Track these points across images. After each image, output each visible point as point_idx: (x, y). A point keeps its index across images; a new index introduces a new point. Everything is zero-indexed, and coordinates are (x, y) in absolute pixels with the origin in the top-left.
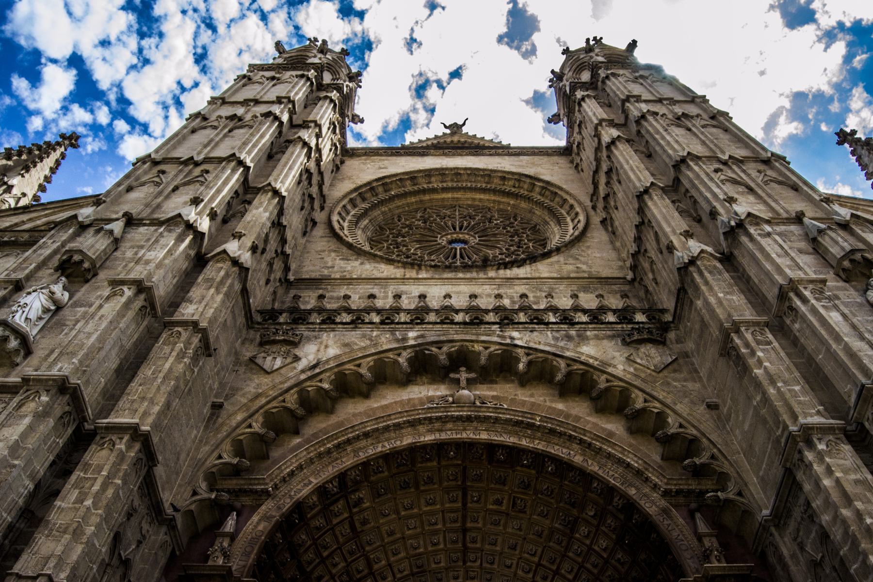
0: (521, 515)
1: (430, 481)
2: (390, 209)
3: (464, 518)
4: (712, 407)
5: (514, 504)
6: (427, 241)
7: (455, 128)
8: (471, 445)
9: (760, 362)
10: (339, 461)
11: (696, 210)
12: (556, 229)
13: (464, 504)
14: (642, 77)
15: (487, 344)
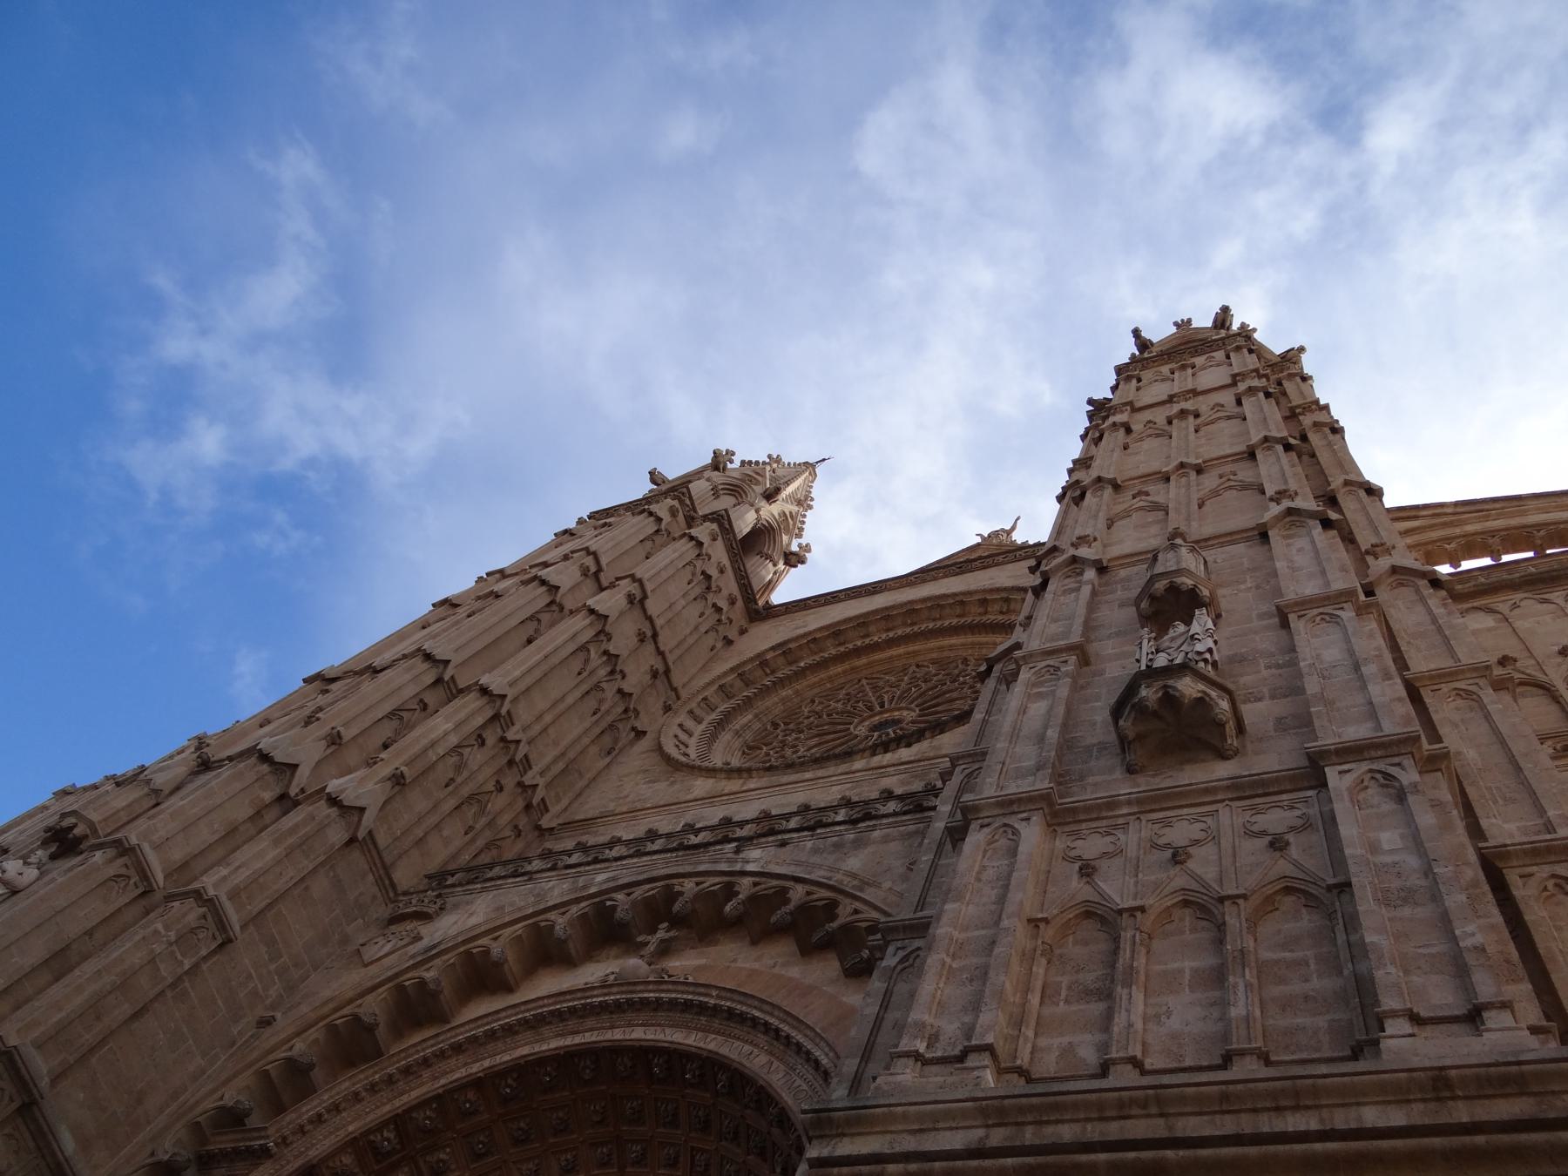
2: (797, 693)
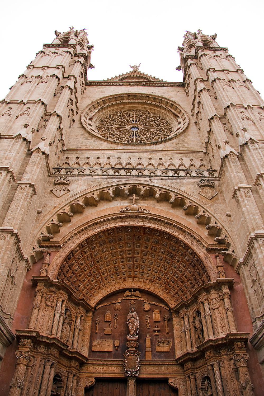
0: (155, 253)
1: (121, 239)
3: (133, 253)
4: (228, 215)
5: (152, 248)
6: (122, 128)
7: (136, 68)
8: (137, 227)
9: (245, 205)
10: (86, 234)
11: (232, 129)
13: (134, 248)
14: (217, 56)
15: (144, 185)
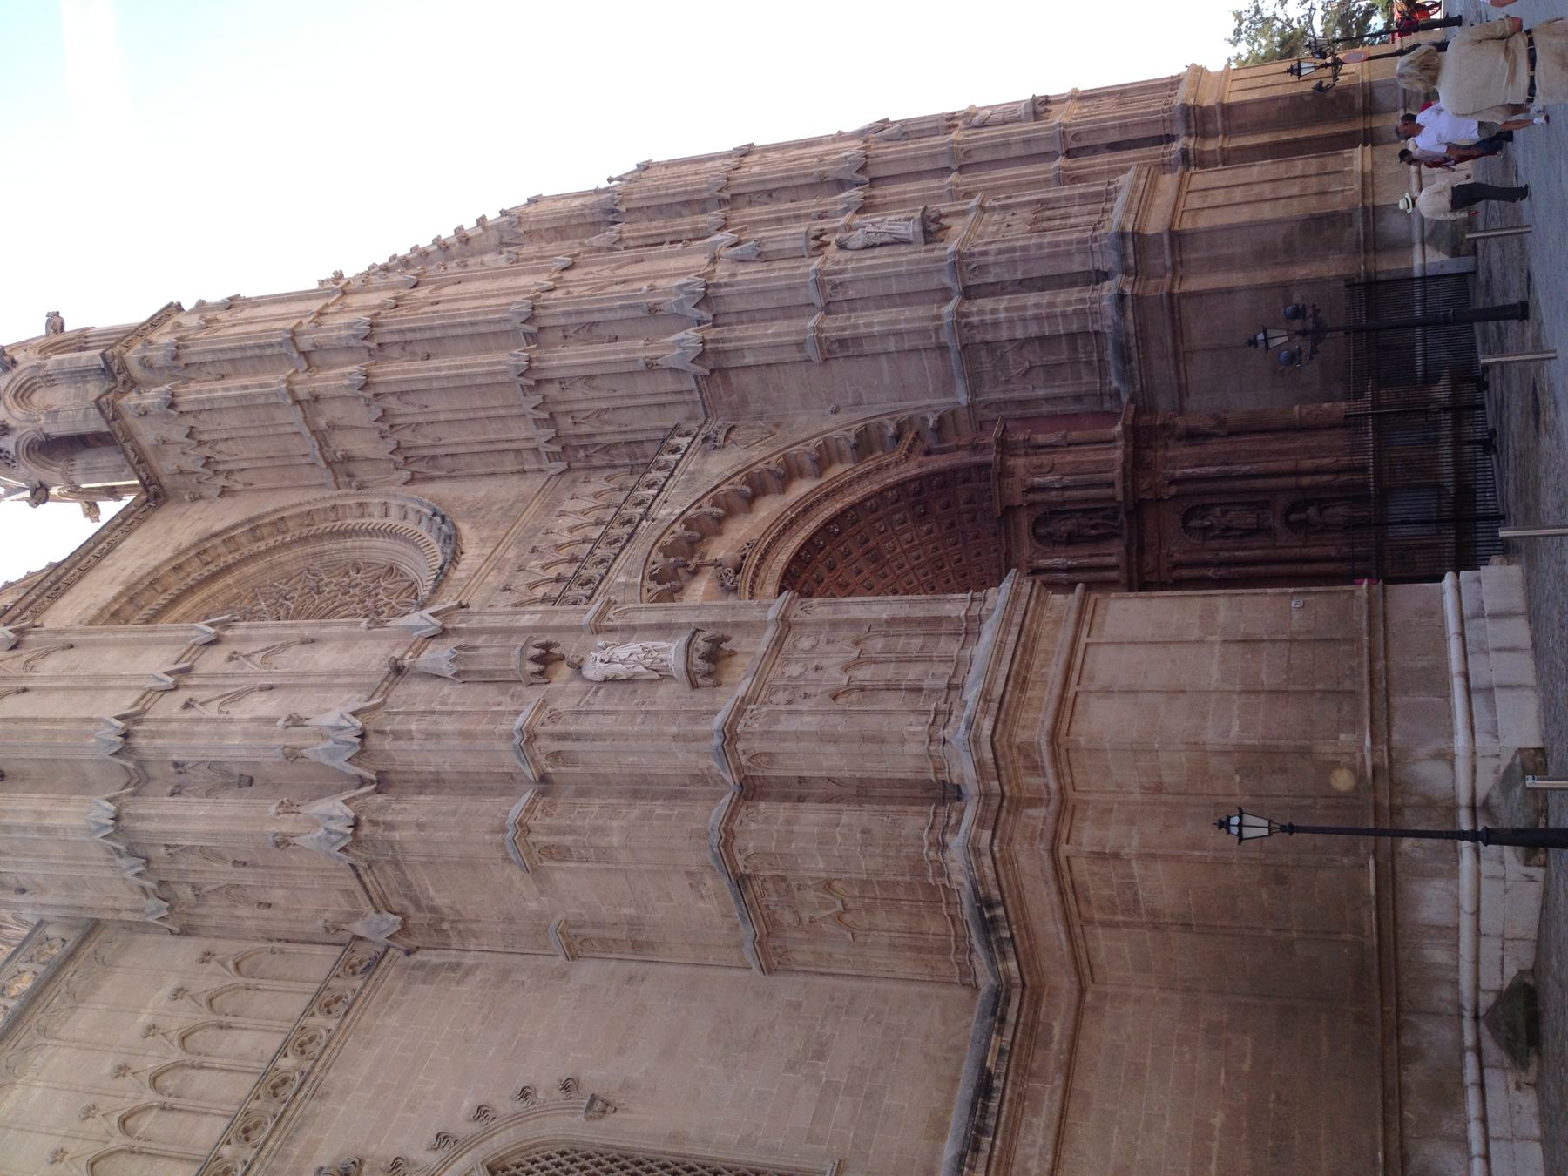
12: (349, 543)
